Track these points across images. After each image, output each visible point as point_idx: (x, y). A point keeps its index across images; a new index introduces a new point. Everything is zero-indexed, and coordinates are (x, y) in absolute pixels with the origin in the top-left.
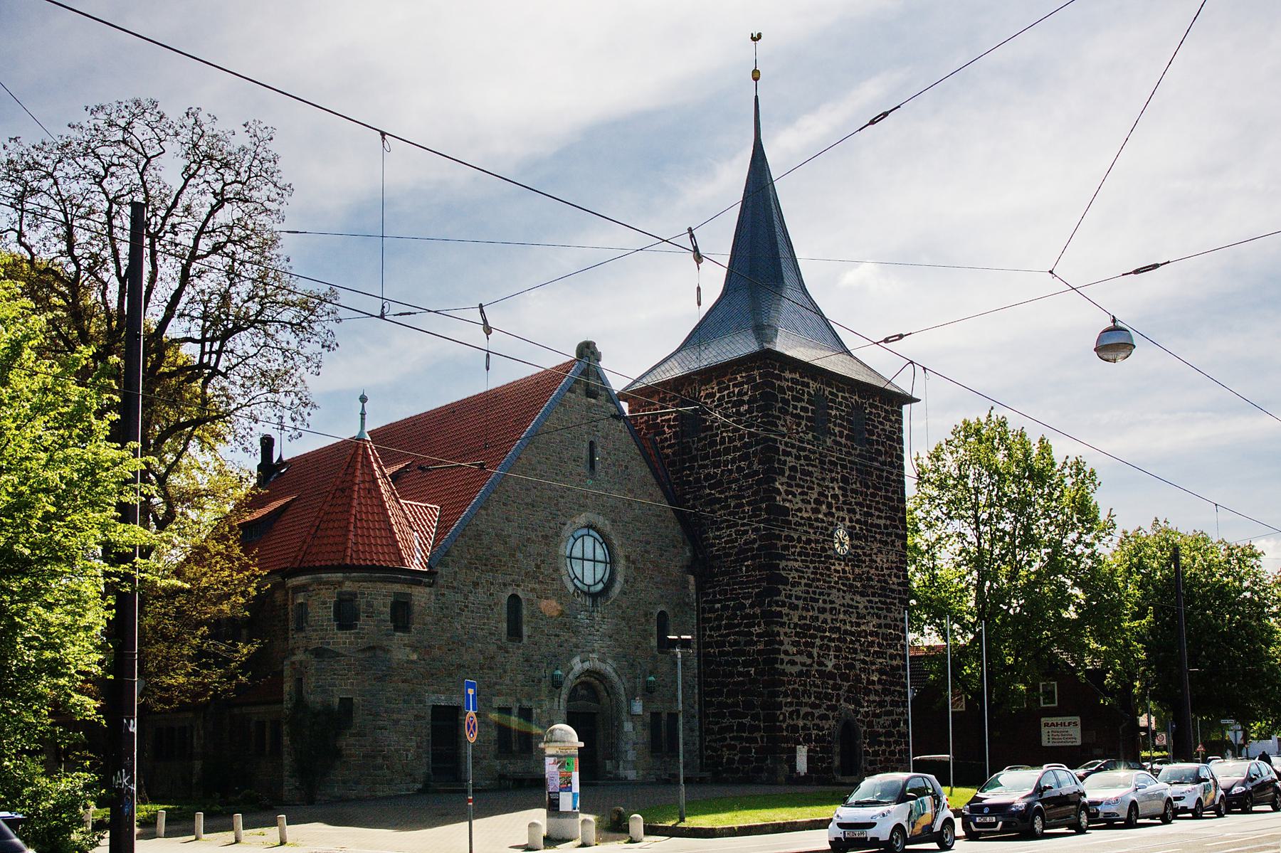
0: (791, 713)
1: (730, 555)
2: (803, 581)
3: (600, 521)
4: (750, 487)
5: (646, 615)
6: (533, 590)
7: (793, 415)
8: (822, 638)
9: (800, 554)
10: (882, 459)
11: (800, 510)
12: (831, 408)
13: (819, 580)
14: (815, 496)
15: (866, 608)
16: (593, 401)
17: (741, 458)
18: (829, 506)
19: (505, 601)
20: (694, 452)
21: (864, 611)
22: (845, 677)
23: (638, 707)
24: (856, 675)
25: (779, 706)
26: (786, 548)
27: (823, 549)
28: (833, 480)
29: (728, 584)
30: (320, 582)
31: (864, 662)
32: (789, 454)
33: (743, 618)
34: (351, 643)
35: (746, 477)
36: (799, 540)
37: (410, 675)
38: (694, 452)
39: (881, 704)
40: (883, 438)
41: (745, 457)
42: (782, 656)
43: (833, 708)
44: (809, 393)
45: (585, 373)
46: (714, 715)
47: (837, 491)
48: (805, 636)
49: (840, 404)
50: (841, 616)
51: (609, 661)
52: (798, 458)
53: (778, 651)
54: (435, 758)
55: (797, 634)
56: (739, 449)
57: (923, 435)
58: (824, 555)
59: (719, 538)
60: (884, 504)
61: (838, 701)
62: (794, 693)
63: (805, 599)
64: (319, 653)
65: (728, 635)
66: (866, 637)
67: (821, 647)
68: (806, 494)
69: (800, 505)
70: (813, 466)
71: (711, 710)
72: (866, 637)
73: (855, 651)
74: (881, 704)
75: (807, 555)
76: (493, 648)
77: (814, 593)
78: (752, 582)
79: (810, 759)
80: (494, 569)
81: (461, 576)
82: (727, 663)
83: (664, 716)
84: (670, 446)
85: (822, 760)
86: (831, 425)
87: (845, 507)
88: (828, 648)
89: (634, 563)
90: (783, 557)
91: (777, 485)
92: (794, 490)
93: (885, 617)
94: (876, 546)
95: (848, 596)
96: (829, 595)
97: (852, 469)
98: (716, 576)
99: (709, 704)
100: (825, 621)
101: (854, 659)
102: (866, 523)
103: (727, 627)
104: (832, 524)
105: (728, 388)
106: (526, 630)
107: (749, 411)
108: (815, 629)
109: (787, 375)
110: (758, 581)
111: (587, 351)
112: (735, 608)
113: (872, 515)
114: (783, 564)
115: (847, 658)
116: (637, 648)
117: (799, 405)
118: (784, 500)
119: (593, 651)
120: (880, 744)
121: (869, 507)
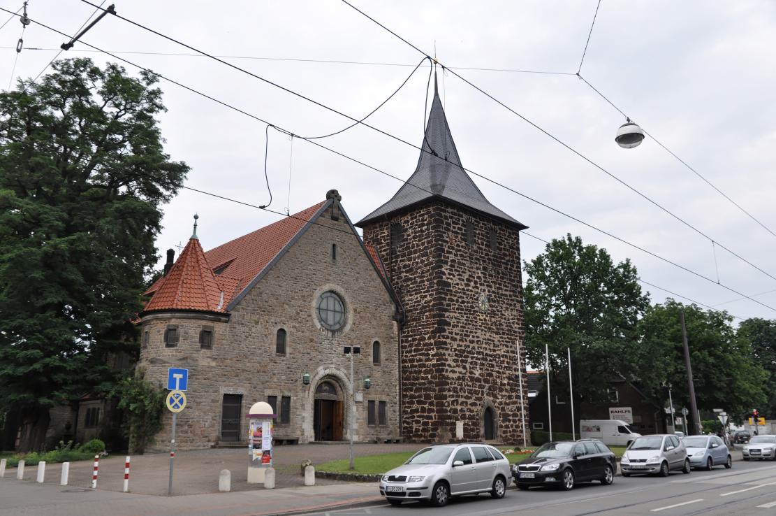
0: (453, 402)
1: (417, 309)
2: (460, 325)
3: (339, 289)
4: (428, 271)
5: (366, 343)
6: (294, 327)
7: (453, 232)
8: (472, 358)
9: (457, 309)
10: (507, 258)
11: (457, 284)
12: (476, 229)
13: (470, 324)
14: (467, 277)
15: (499, 341)
16: (336, 222)
18: (476, 283)
19: (276, 332)
20: (398, 253)
21: (498, 343)
22: (487, 381)
23: (359, 397)
24: (494, 380)
25: (445, 397)
26: (449, 305)
27: (472, 307)
28: (477, 268)
29: (416, 326)
30: (157, 319)
31: (498, 372)
32: (451, 253)
33: (424, 345)
34: (173, 355)
35: (426, 265)
36: (457, 301)
37: (210, 375)
38: (398, 253)
39: (510, 397)
40: (507, 247)
42: (447, 367)
43: (480, 399)
44: (463, 221)
45: (331, 206)
46: (408, 403)
47: (480, 275)
48: (461, 356)
49: (482, 227)
50: (484, 345)
51: (342, 369)
52: (456, 255)
53: (444, 365)
54: (225, 426)
55: (456, 355)
57: (531, 248)
58: (472, 311)
59: (410, 300)
60: (508, 283)
61: (482, 395)
62: (455, 390)
63: (461, 335)
64: (152, 362)
65: (416, 355)
66: (499, 358)
67: (471, 363)
68: (461, 275)
69: (458, 281)
70: (465, 260)
71: (406, 400)
72: (499, 358)
73: (493, 366)
74: (510, 397)
75: (462, 310)
76: (266, 360)
77: (467, 331)
78: (430, 324)
79: (465, 430)
80: (269, 313)
81: (247, 317)
82: (415, 372)
83: (377, 403)
84: (385, 251)
85: (473, 430)
86: (476, 239)
87: (485, 284)
88: (476, 364)
89: (359, 313)
90: (446, 310)
91: (443, 269)
92: (454, 273)
93: (511, 347)
94: (505, 306)
95: (488, 334)
96: (476, 333)
97: (489, 263)
99: (405, 396)
100: (474, 348)
101: (492, 371)
102: (498, 293)
103: (415, 350)
104: (477, 293)
105: (416, 217)
106: (288, 350)
107: (428, 229)
108: (468, 352)
109: (450, 210)
110: (433, 324)
111: (333, 196)
112: (419, 340)
113: (501, 289)
114: (447, 314)
115: (487, 370)
116: (360, 362)
117: (457, 226)
118: (447, 278)
119: (332, 363)
120: (509, 421)
121: (500, 284)
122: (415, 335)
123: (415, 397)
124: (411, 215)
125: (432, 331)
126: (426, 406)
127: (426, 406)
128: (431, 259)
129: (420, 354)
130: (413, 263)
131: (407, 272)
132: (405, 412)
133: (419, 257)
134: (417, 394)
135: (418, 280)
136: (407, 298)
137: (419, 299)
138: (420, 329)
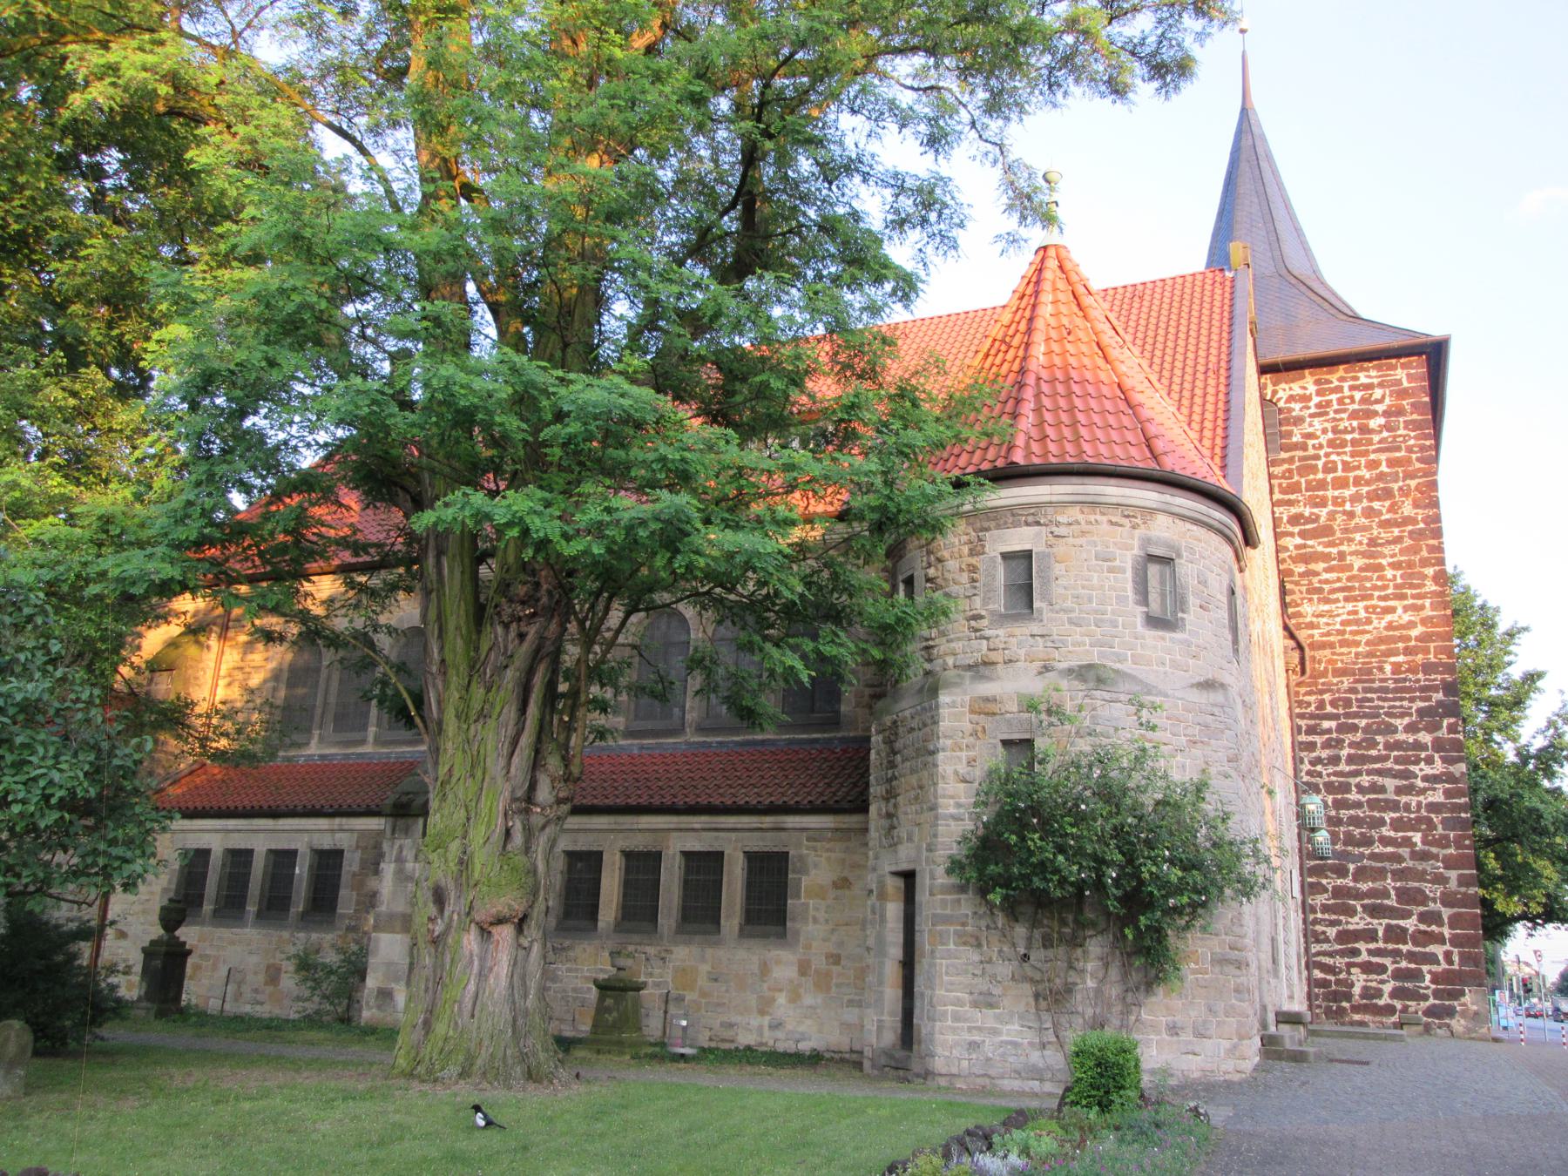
4: (1398, 540)
17: (1372, 496)
33: (1388, 746)
35: (1386, 524)
41: (1388, 494)
46: (1326, 909)
56: (1368, 483)
65: (1357, 773)
71: (1320, 900)
82: (1356, 821)
98: (1324, 674)
99: (1317, 889)
103: (1351, 759)
105: (1339, 389)
110: (1423, 689)
112: (1366, 729)
122: (1347, 715)
123: (1359, 896)
124: (1317, 382)
125: (1419, 711)
126: (1411, 924)
127: (1411, 924)
128: (1407, 509)
129: (1369, 773)
130: (1332, 516)
131: (1302, 534)
132: (1319, 938)
133: (1355, 499)
134: (1364, 887)
135: (1358, 562)
136: (1307, 609)
137: (1362, 614)
138: (1371, 700)
